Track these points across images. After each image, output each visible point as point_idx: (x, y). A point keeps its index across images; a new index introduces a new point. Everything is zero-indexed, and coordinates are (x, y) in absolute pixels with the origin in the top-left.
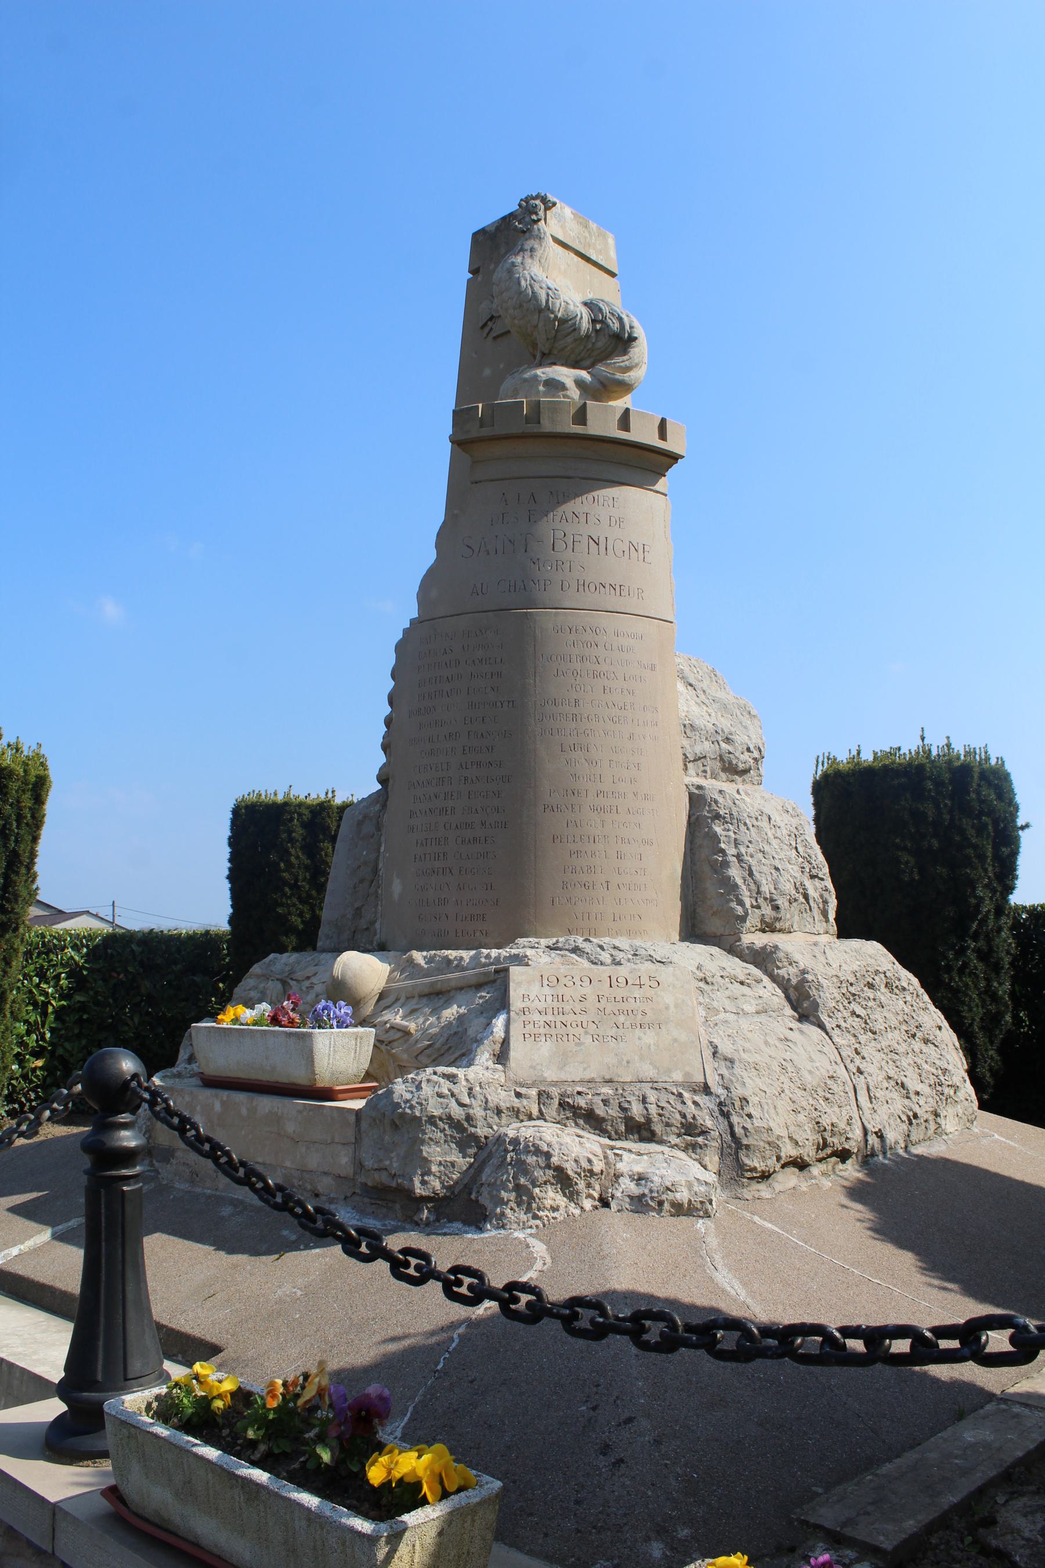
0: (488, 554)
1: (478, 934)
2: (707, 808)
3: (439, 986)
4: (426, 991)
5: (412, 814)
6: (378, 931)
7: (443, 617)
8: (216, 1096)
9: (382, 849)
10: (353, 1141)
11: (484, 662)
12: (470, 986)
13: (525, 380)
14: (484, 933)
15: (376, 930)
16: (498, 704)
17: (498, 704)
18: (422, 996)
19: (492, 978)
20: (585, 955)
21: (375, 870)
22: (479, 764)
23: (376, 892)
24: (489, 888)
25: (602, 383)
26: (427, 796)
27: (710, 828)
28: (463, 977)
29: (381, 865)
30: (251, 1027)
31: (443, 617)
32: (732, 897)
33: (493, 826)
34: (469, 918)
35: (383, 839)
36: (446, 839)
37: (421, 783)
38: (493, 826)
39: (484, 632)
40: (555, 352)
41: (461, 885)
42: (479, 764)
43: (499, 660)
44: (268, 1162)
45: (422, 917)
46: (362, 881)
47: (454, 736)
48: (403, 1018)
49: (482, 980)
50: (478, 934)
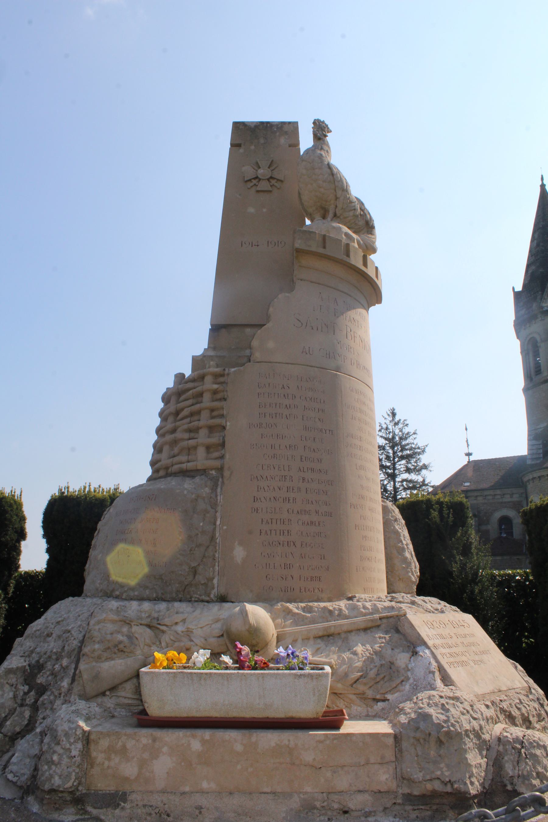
0: (312, 329)
1: (316, 591)
2: (390, 514)
3: (332, 630)
4: (321, 634)
5: (255, 499)
6: (216, 586)
7: (279, 363)
8: (194, 736)
9: (218, 523)
10: (394, 759)
11: (313, 400)
12: (359, 630)
13: (334, 228)
14: (321, 590)
15: (214, 585)
16: (324, 431)
17: (324, 431)
18: (317, 637)
19: (379, 622)
20: (421, 607)
21: (213, 538)
22: (312, 470)
23: (214, 556)
24: (323, 558)
25: (366, 246)
26: (272, 488)
27: (394, 527)
28: (354, 623)
29: (217, 535)
30: (202, 671)
31: (279, 363)
32: (409, 570)
33: (324, 515)
34: (309, 579)
35: (218, 515)
36: (290, 520)
37: (264, 477)
38: (324, 515)
39: (312, 380)
40: (342, 217)
41: (303, 555)
42: (312, 470)
43: (322, 401)
44: (279, 790)
45: (268, 576)
46: (199, 546)
47: (293, 448)
48: (313, 655)
49: (370, 625)
50: (316, 591)
